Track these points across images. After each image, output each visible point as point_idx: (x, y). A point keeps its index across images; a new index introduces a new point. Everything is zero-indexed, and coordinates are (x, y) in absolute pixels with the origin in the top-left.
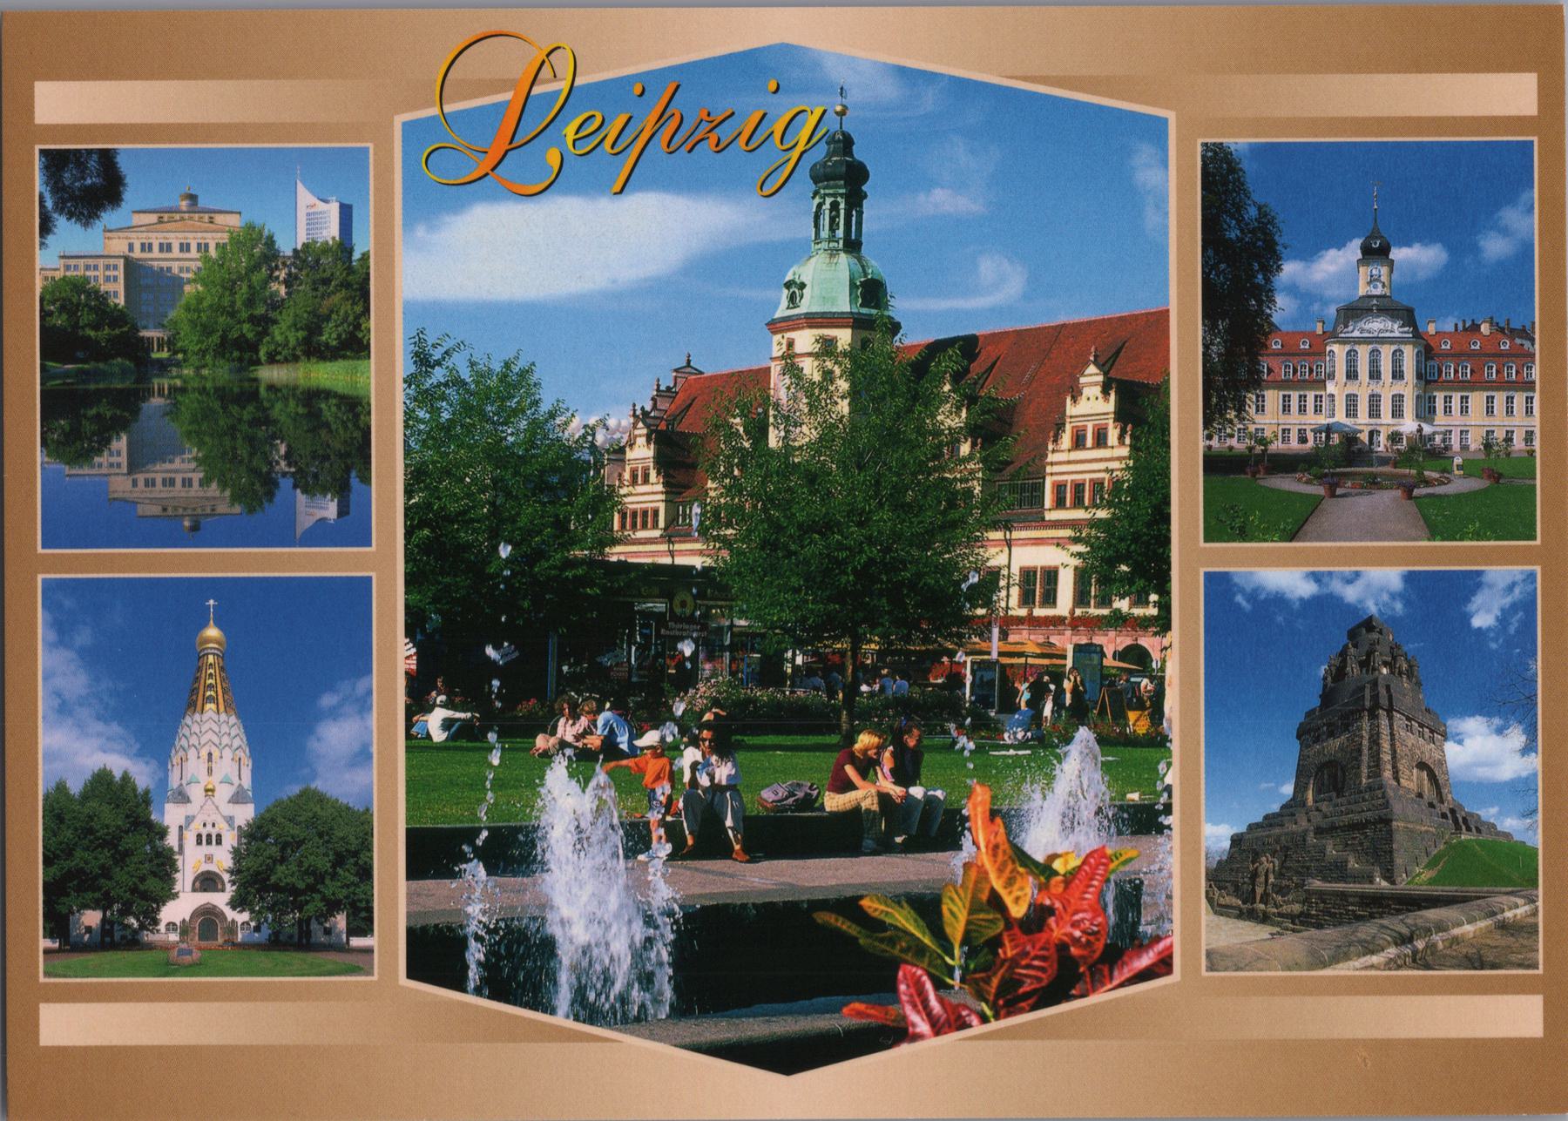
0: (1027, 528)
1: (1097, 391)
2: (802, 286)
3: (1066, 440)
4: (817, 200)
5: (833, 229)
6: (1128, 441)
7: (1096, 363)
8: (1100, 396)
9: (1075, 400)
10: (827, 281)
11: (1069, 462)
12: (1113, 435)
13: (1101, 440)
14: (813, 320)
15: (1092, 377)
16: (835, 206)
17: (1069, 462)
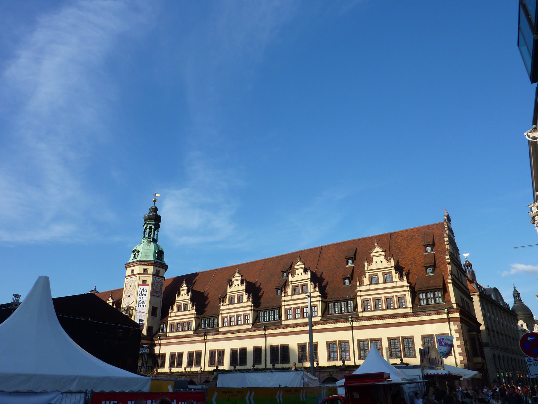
0: (213, 335)
1: (239, 282)
2: (139, 252)
3: (227, 301)
4: (145, 226)
5: (149, 235)
6: (251, 299)
7: (238, 272)
8: (240, 284)
9: (231, 286)
10: (147, 251)
11: (228, 309)
12: (245, 297)
13: (240, 300)
14: (141, 263)
15: (237, 279)
16: (151, 228)
17: (228, 309)
